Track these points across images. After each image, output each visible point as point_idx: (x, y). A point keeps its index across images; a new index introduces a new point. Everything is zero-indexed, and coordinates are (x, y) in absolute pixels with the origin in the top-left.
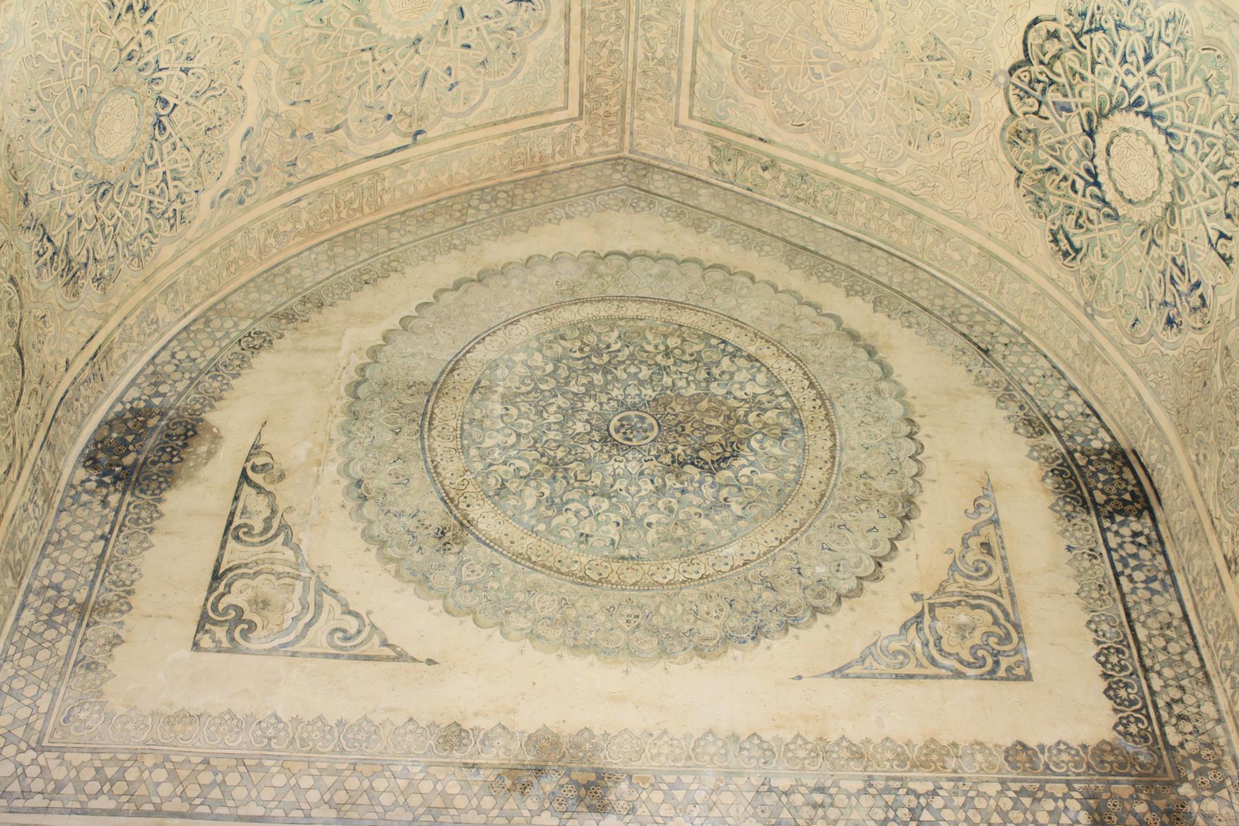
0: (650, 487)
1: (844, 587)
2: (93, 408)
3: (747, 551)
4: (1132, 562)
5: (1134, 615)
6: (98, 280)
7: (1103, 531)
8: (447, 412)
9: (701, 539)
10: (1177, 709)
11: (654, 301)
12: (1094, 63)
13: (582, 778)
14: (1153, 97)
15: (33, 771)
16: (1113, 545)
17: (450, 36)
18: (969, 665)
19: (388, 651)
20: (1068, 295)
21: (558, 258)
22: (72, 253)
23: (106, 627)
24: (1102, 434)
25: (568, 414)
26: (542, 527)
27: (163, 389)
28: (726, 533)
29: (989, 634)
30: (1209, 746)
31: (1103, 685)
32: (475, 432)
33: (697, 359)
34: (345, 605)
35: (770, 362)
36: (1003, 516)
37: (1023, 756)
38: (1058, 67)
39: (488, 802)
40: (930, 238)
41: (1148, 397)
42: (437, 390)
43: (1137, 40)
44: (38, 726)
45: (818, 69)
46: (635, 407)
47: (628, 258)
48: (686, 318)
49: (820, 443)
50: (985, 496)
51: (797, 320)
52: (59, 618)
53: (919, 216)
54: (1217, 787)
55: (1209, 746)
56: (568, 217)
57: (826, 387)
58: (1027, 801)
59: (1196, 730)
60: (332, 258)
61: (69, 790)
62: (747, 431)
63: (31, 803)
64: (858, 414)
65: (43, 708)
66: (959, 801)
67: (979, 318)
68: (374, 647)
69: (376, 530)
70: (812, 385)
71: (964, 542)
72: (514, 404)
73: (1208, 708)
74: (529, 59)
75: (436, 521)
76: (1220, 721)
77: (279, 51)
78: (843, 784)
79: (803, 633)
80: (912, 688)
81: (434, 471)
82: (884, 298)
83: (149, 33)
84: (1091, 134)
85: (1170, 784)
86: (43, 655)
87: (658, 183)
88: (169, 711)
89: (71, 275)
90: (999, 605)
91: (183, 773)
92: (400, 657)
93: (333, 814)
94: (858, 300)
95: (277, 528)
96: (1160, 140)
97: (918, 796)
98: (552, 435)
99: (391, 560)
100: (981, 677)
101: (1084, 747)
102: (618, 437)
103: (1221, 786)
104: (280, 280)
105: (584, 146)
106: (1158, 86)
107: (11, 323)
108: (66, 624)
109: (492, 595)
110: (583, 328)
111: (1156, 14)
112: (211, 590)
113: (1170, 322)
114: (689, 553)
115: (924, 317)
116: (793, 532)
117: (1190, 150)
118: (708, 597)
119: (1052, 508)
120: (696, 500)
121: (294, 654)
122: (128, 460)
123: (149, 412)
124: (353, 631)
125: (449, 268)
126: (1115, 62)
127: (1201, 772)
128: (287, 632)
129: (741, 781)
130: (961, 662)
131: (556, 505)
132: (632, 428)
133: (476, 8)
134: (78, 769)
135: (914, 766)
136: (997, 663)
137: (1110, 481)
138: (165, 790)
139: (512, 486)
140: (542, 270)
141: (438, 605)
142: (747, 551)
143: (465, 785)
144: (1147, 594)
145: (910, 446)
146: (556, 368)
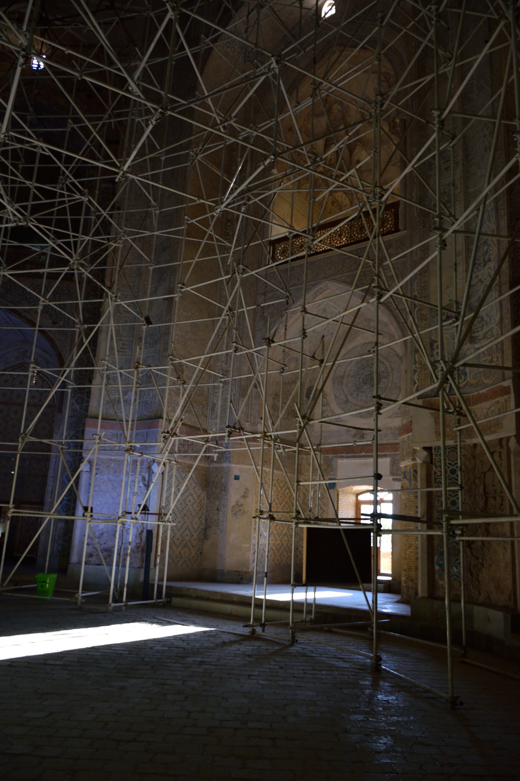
25: (359, 378)
81: (344, 391)
95: (328, 404)
131: (358, 395)
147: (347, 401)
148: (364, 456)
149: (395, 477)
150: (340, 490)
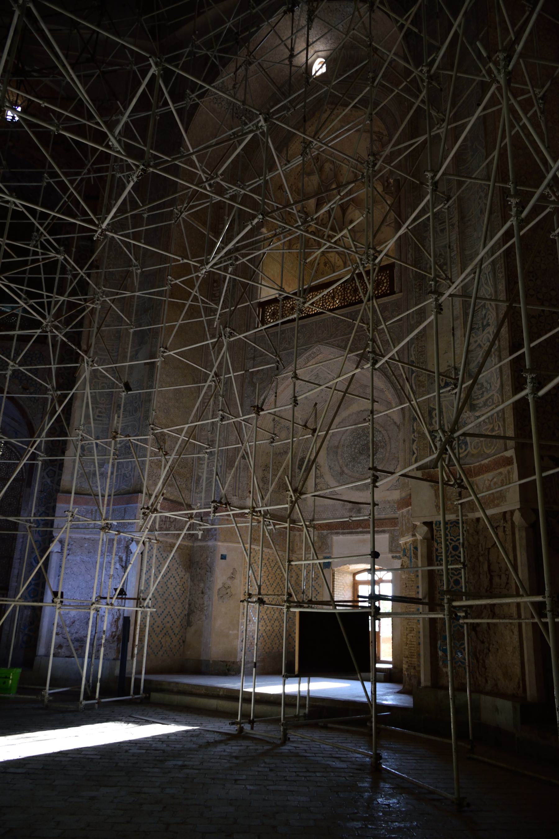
25: (355, 448)
42: (338, 447)
46: (363, 445)
75: (339, 471)
95: (322, 476)
131: (354, 466)
147: (342, 473)
148: (361, 532)
149: (394, 555)
150: (336, 569)
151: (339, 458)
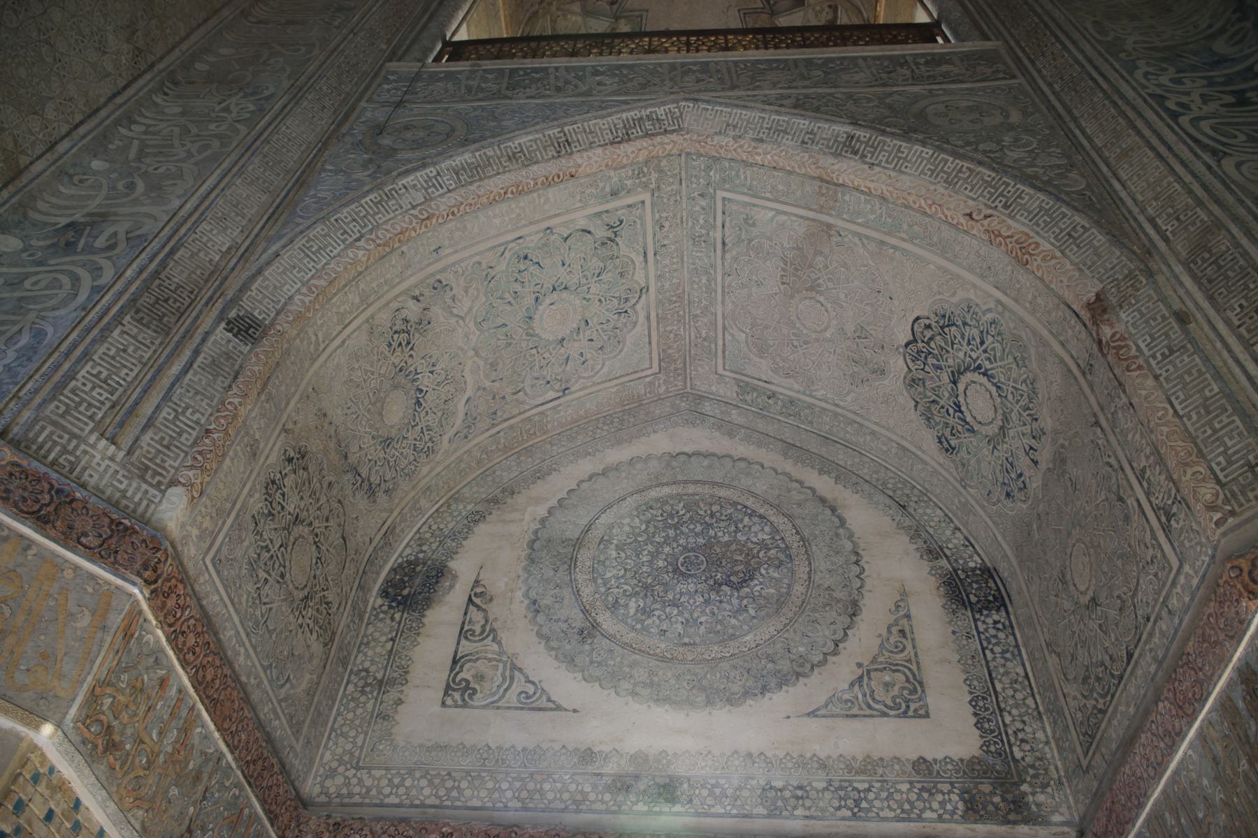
0: (701, 599)
1: (816, 659)
2: (386, 562)
3: (758, 638)
4: (994, 641)
5: (994, 675)
6: (386, 492)
7: (975, 620)
8: (585, 557)
9: (731, 631)
10: (1020, 735)
11: (704, 483)
12: (953, 343)
13: (661, 781)
14: (987, 365)
15: (354, 781)
16: (981, 629)
17: (581, 336)
18: (891, 708)
19: (551, 705)
20: (951, 473)
21: (649, 457)
22: (372, 480)
23: (393, 694)
24: (976, 558)
25: (654, 556)
26: (639, 626)
27: (424, 548)
28: (745, 627)
29: (903, 688)
30: (1040, 759)
31: (974, 720)
32: (601, 569)
33: (730, 518)
34: (527, 677)
35: (772, 519)
36: (913, 612)
37: (923, 767)
38: (932, 344)
39: (607, 797)
40: (868, 438)
41: (1000, 538)
42: (578, 543)
43: (975, 332)
44: (357, 754)
45: (796, 343)
46: (693, 550)
47: (689, 456)
48: (723, 493)
49: (802, 569)
50: (902, 600)
51: (789, 491)
52: (368, 689)
53: (861, 425)
54: (1044, 786)
55: (1040, 759)
56: (655, 432)
57: (806, 533)
58: (926, 795)
59: (1032, 749)
60: (519, 464)
61: (374, 792)
62: (758, 563)
63: (353, 801)
64: (825, 550)
65: (359, 744)
66: (884, 795)
67: (900, 485)
68: (543, 703)
69: (545, 630)
70: (797, 533)
71: (889, 629)
72: (623, 551)
73: (1040, 735)
74: (628, 343)
76: (1047, 743)
77: (483, 355)
78: (814, 784)
79: (791, 689)
80: (856, 724)
81: (577, 593)
82: (841, 475)
83: (411, 356)
84: (955, 383)
85: (1015, 783)
86: (359, 711)
87: (707, 408)
88: (429, 744)
89: (371, 493)
90: (910, 669)
91: (437, 781)
92: (559, 708)
93: (520, 805)
94: (826, 477)
95: (489, 631)
96: (994, 389)
97: (859, 792)
98: (645, 569)
99: (553, 649)
100: (898, 716)
101: (962, 760)
102: (683, 569)
103: (1048, 785)
104: (490, 478)
105: (663, 388)
106: (989, 359)
107: (339, 525)
108: (371, 692)
109: (610, 669)
110: (663, 501)
111: (984, 319)
112: (452, 669)
113: (1008, 495)
114: (724, 641)
115: (866, 487)
116: (785, 626)
117: (1010, 397)
118: (735, 668)
119: (943, 607)
120: (728, 607)
121: (498, 708)
122: (405, 592)
123: (417, 562)
124: (531, 693)
125: (586, 466)
126: (965, 344)
127: (1034, 776)
128: (494, 694)
129: (754, 782)
130: (886, 706)
131: (646, 612)
132: (691, 563)
133: (595, 319)
134: (379, 780)
135: (857, 773)
136: (908, 707)
137: (980, 588)
138: (427, 792)
139: (622, 602)
140: (639, 466)
141: (579, 676)
142: (758, 638)
143: (595, 786)
144: (1003, 661)
145: (856, 569)
146: (647, 527)
151: (581, 577)
